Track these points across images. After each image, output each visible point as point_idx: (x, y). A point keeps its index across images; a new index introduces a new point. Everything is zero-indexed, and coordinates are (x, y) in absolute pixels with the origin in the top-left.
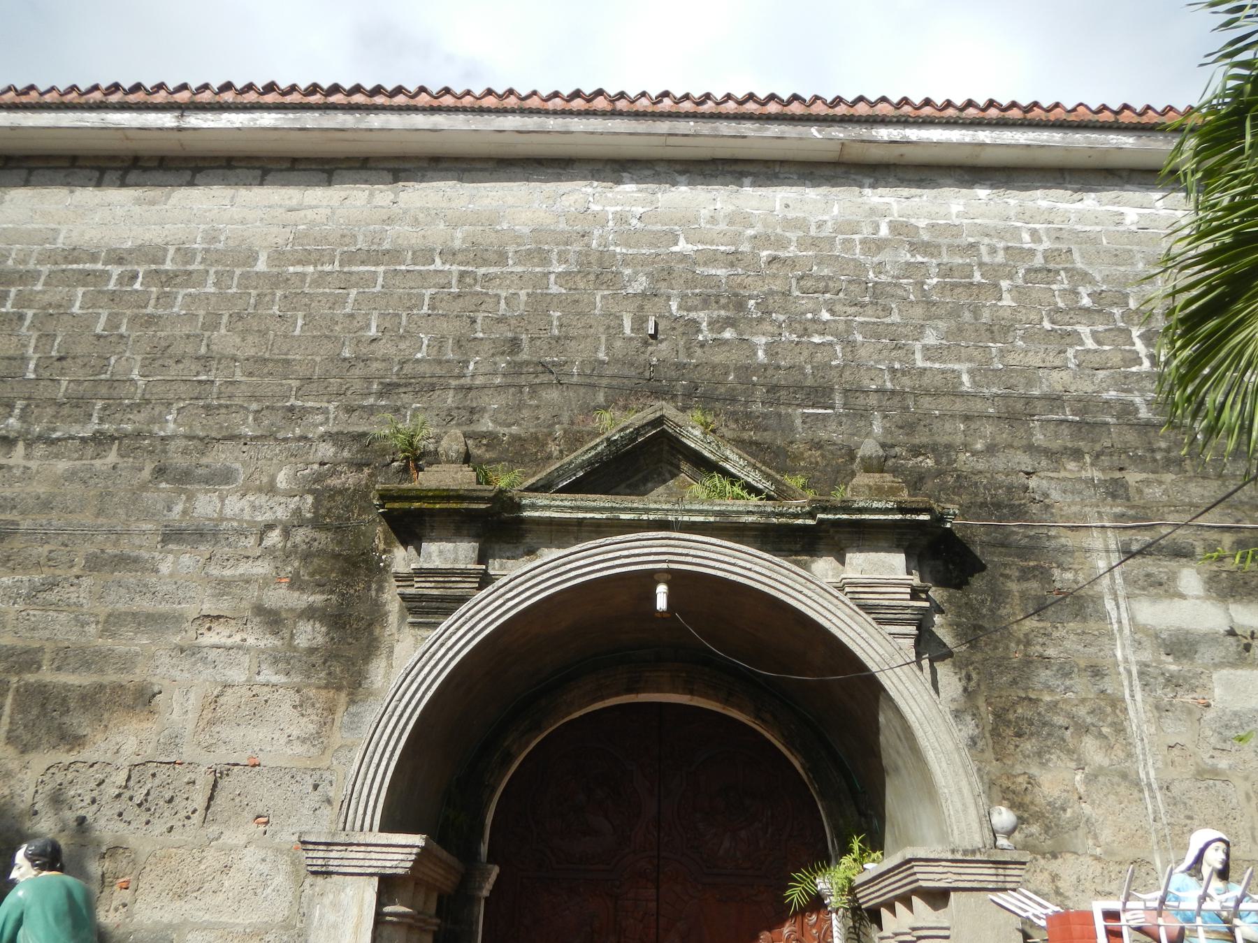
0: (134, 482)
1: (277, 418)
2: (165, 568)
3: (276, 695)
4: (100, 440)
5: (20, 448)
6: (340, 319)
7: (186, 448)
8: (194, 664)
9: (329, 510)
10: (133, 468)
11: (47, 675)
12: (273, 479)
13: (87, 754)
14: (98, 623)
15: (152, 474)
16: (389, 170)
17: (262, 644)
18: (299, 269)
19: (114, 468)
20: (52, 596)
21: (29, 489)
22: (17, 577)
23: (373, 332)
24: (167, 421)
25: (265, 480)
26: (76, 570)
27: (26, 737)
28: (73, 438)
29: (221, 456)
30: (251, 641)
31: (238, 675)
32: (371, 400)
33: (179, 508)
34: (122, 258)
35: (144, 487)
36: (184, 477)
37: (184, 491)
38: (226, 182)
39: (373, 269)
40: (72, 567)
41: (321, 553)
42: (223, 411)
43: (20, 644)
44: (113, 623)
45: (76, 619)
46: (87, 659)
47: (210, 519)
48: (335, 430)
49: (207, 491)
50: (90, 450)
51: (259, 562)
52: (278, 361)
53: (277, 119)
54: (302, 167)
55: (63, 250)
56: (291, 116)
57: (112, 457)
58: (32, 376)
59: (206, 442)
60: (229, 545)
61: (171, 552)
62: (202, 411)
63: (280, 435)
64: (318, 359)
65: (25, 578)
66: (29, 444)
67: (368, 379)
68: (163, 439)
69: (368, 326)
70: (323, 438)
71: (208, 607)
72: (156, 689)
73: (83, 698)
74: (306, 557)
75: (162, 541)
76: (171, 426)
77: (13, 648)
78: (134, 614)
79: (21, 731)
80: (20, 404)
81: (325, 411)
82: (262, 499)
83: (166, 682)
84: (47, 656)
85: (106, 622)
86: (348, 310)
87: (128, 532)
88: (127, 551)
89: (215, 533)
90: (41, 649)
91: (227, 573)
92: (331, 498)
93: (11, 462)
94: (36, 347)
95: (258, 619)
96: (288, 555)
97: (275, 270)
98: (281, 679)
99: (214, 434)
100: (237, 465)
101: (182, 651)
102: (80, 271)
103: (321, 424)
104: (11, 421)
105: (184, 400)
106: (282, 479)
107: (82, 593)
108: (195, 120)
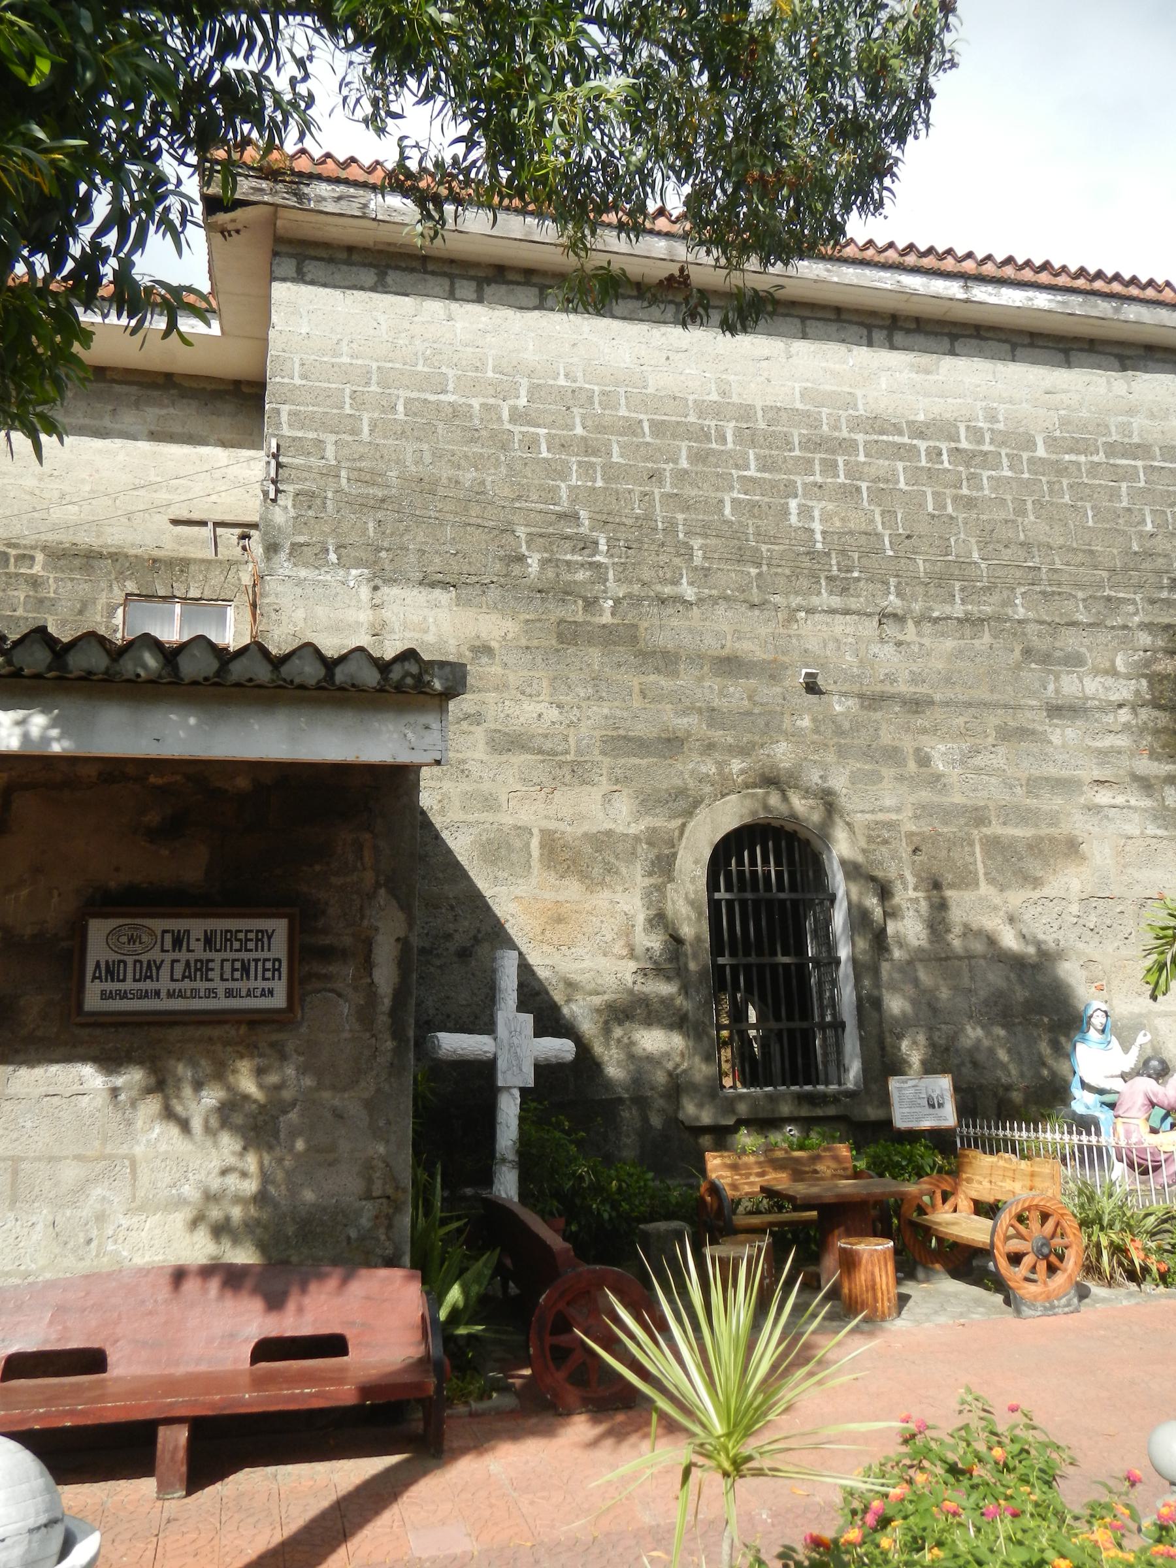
0: (1010, 662)
1: (1100, 606)
2: (1056, 739)
3: (1161, 845)
4: (966, 620)
5: (910, 623)
6: (1120, 512)
7: (1040, 631)
8: (1101, 820)
9: (1161, 692)
10: (1006, 648)
11: (996, 829)
12: (1113, 662)
13: (1047, 891)
14: (1021, 786)
15: (1022, 655)
16: (1117, 356)
17: (1138, 804)
18: (1073, 457)
19: (991, 648)
20: (978, 761)
21: (930, 665)
22: (949, 745)
23: (1149, 527)
24: (1016, 605)
25: (1108, 664)
26: (991, 740)
27: (1000, 879)
28: (949, 618)
29: (1071, 641)
30: (1133, 802)
31: (1133, 829)
32: (1164, 594)
33: (1051, 687)
34: (922, 432)
35: (1018, 667)
36: (1046, 659)
37: (1050, 672)
38: (981, 354)
39: (1133, 463)
40: (987, 736)
41: (1165, 730)
42: (1057, 597)
43: (969, 803)
44: (1034, 785)
45: (1003, 781)
46: (1025, 816)
47: (1077, 698)
48: (1147, 620)
49: (1068, 673)
50: (968, 630)
51: (1119, 736)
52: (1084, 551)
53: (1050, 301)
54: (1040, 343)
55: (868, 418)
56: (1059, 298)
57: (987, 638)
58: (891, 553)
59: (1054, 627)
60: (1096, 720)
61: (1056, 726)
62: (1040, 596)
63: (1109, 623)
64: (1115, 551)
65: (955, 746)
66: (917, 623)
67: (1158, 573)
68: (1019, 622)
69: (1144, 521)
70: (1143, 626)
71: (1097, 774)
72: (1080, 840)
73: (1030, 847)
74: (1156, 732)
75: (1049, 716)
76: (1021, 610)
77: (965, 806)
78: (1047, 779)
79: (994, 874)
80: (893, 581)
81: (1134, 602)
82: (1109, 681)
83: (1085, 835)
84: (993, 813)
85: (1028, 784)
86: (1125, 504)
87: (1020, 707)
88: (1025, 724)
89: (1086, 710)
90: (986, 807)
91: (1099, 744)
92: (1160, 681)
93: (908, 638)
94: (883, 523)
95: (1136, 785)
96: (1143, 730)
97: (1054, 457)
98: (1160, 832)
99: (1057, 620)
100: (1083, 650)
101: (1090, 810)
102: (894, 444)
103: (1134, 614)
104: (892, 597)
105: (1024, 585)
106: (1119, 662)
107: (998, 758)
108: (982, 294)
